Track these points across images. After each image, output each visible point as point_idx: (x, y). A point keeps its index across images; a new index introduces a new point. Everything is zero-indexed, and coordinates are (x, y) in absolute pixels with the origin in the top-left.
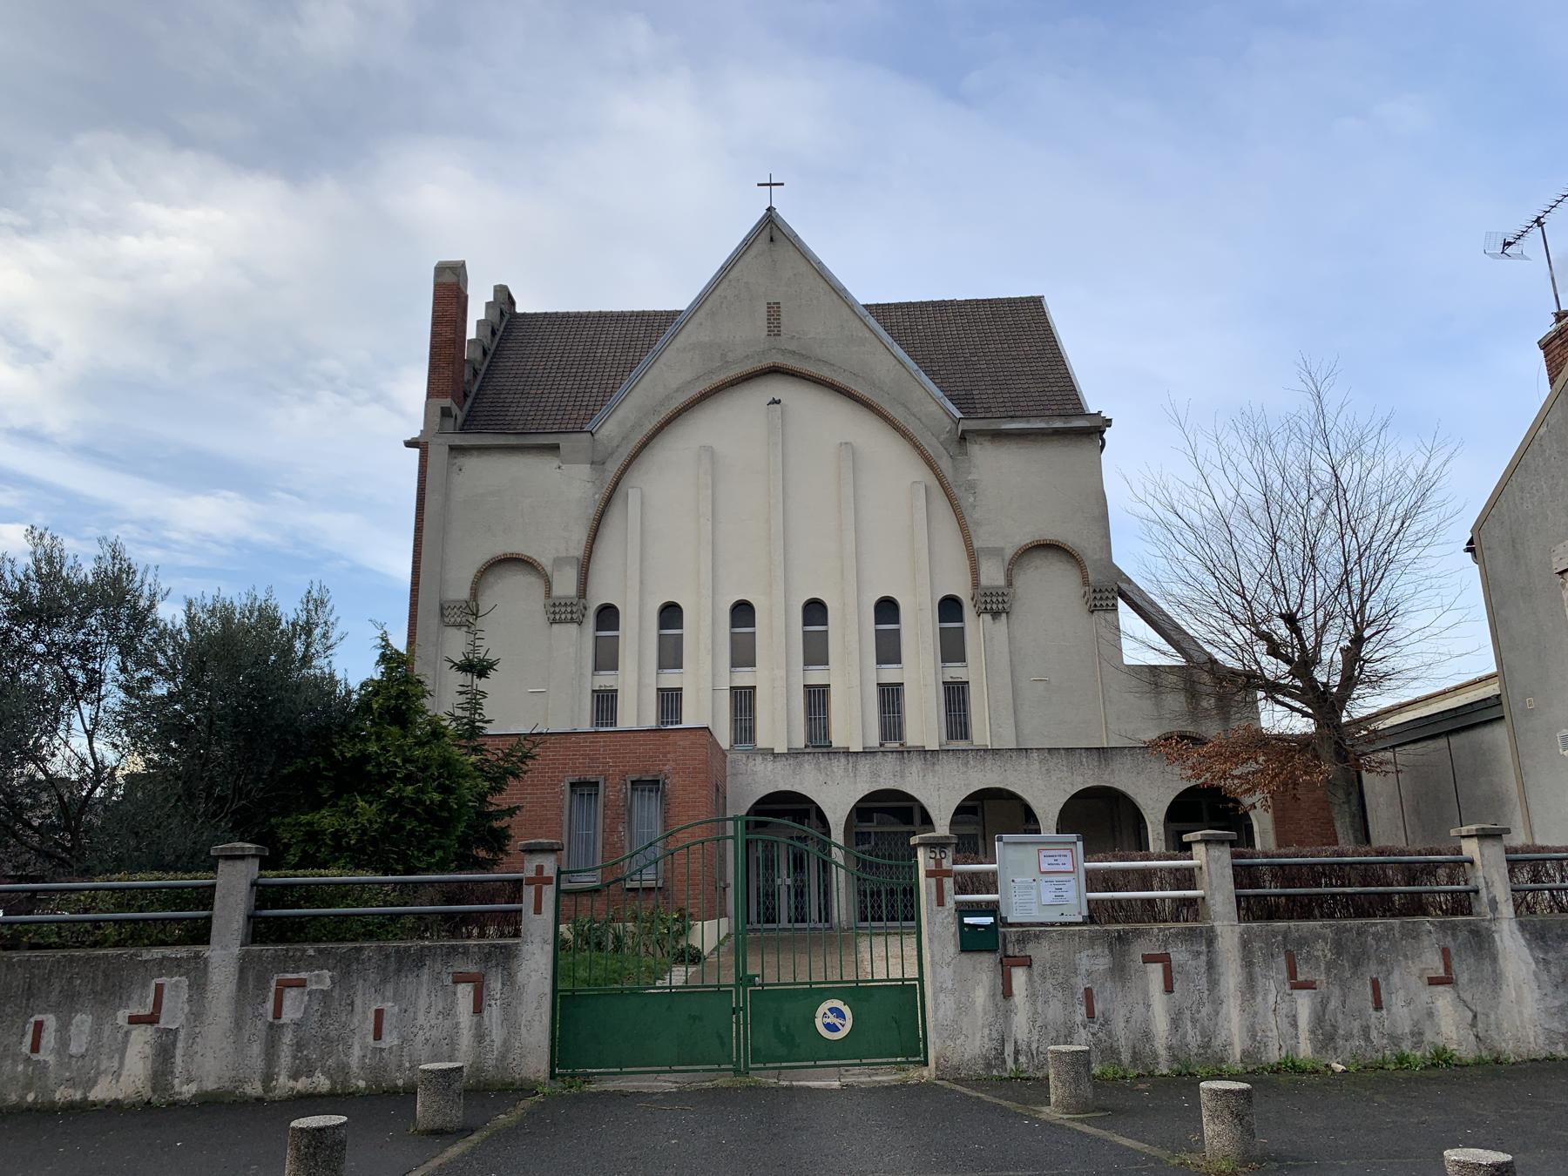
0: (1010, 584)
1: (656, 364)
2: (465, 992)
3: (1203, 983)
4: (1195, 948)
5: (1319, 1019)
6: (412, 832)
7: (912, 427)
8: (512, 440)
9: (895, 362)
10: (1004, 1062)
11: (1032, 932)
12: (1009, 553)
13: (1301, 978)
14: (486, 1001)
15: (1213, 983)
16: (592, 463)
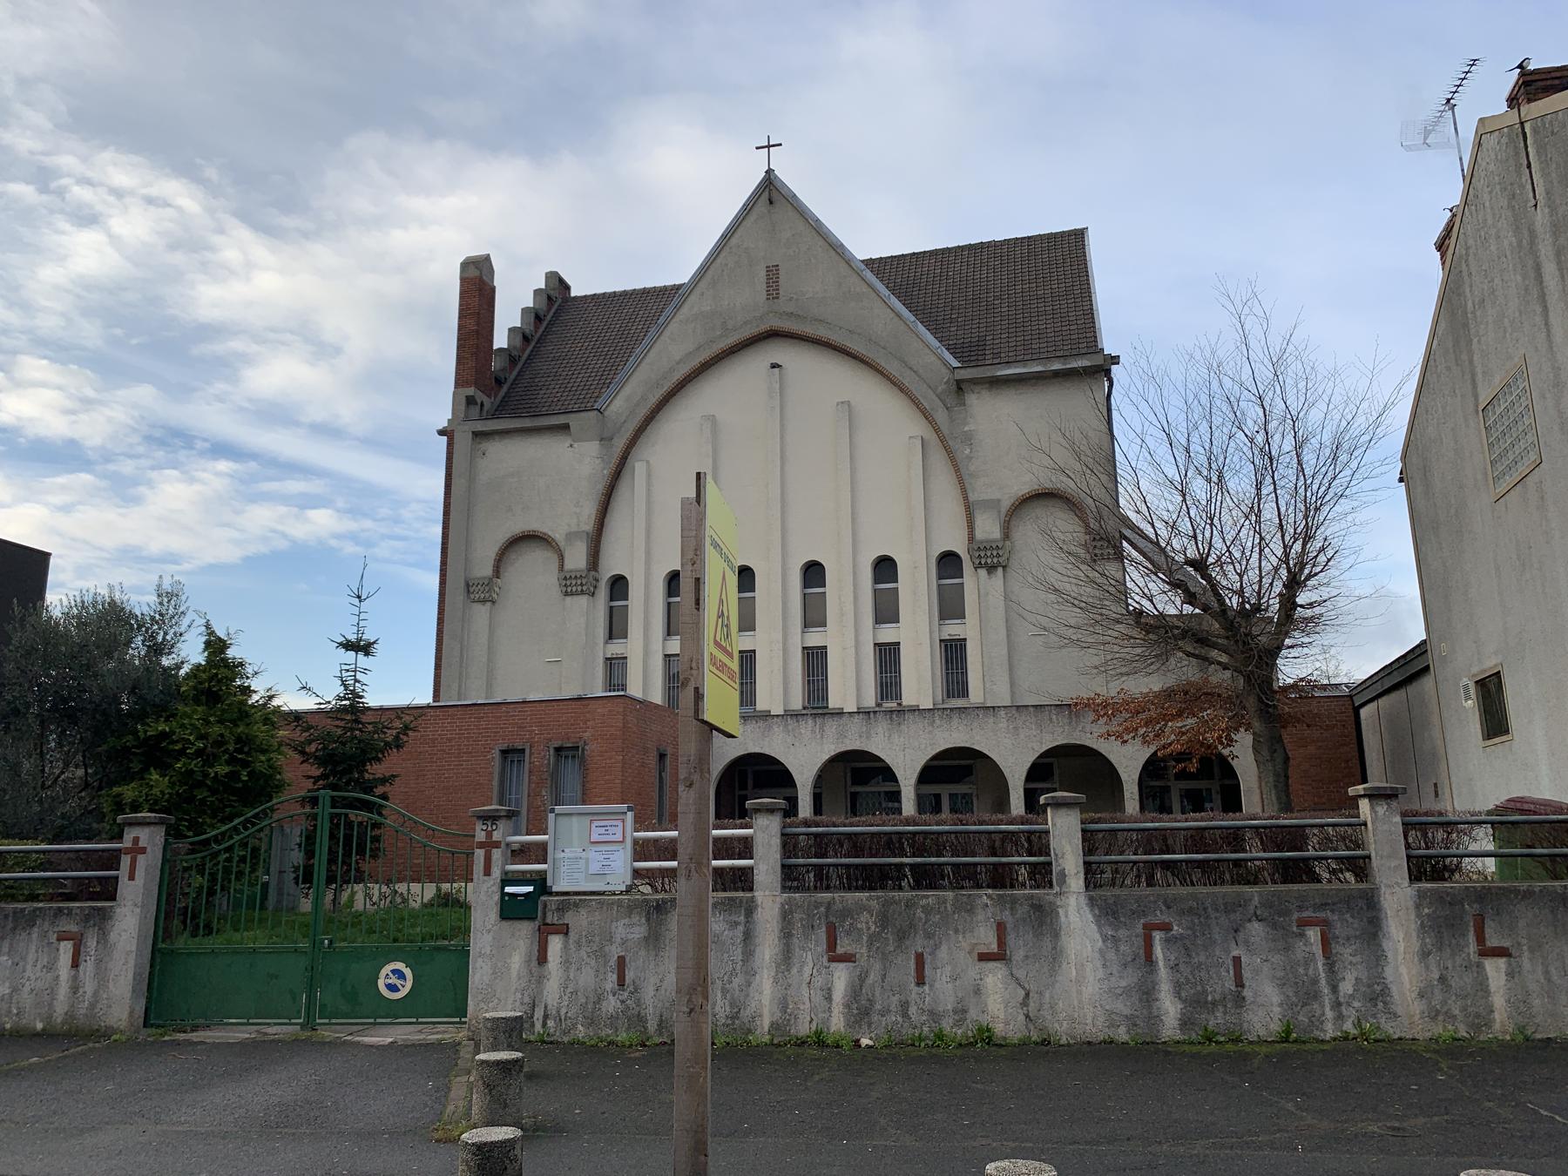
0: (1006, 535)
1: (662, 338)
2: (66, 948)
3: (738, 954)
4: (734, 918)
5: (855, 992)
6: (203, 801)
7: (908, 380)
8: (528, 423)
9: (893, 315)
10: (533, 1025)
11: (574, 900)
12: (1006, 504)
13: (840, 950)
14: (82, 958)
15: (748, 954)
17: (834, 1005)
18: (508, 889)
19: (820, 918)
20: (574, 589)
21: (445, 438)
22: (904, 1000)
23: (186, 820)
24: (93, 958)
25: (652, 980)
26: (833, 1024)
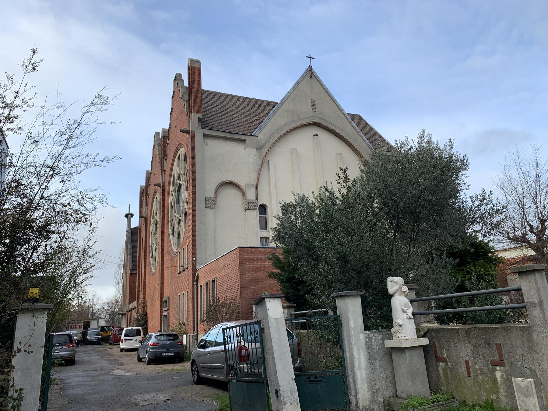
9: (352, 127)
16: (257, 149)
20: (252, 207)
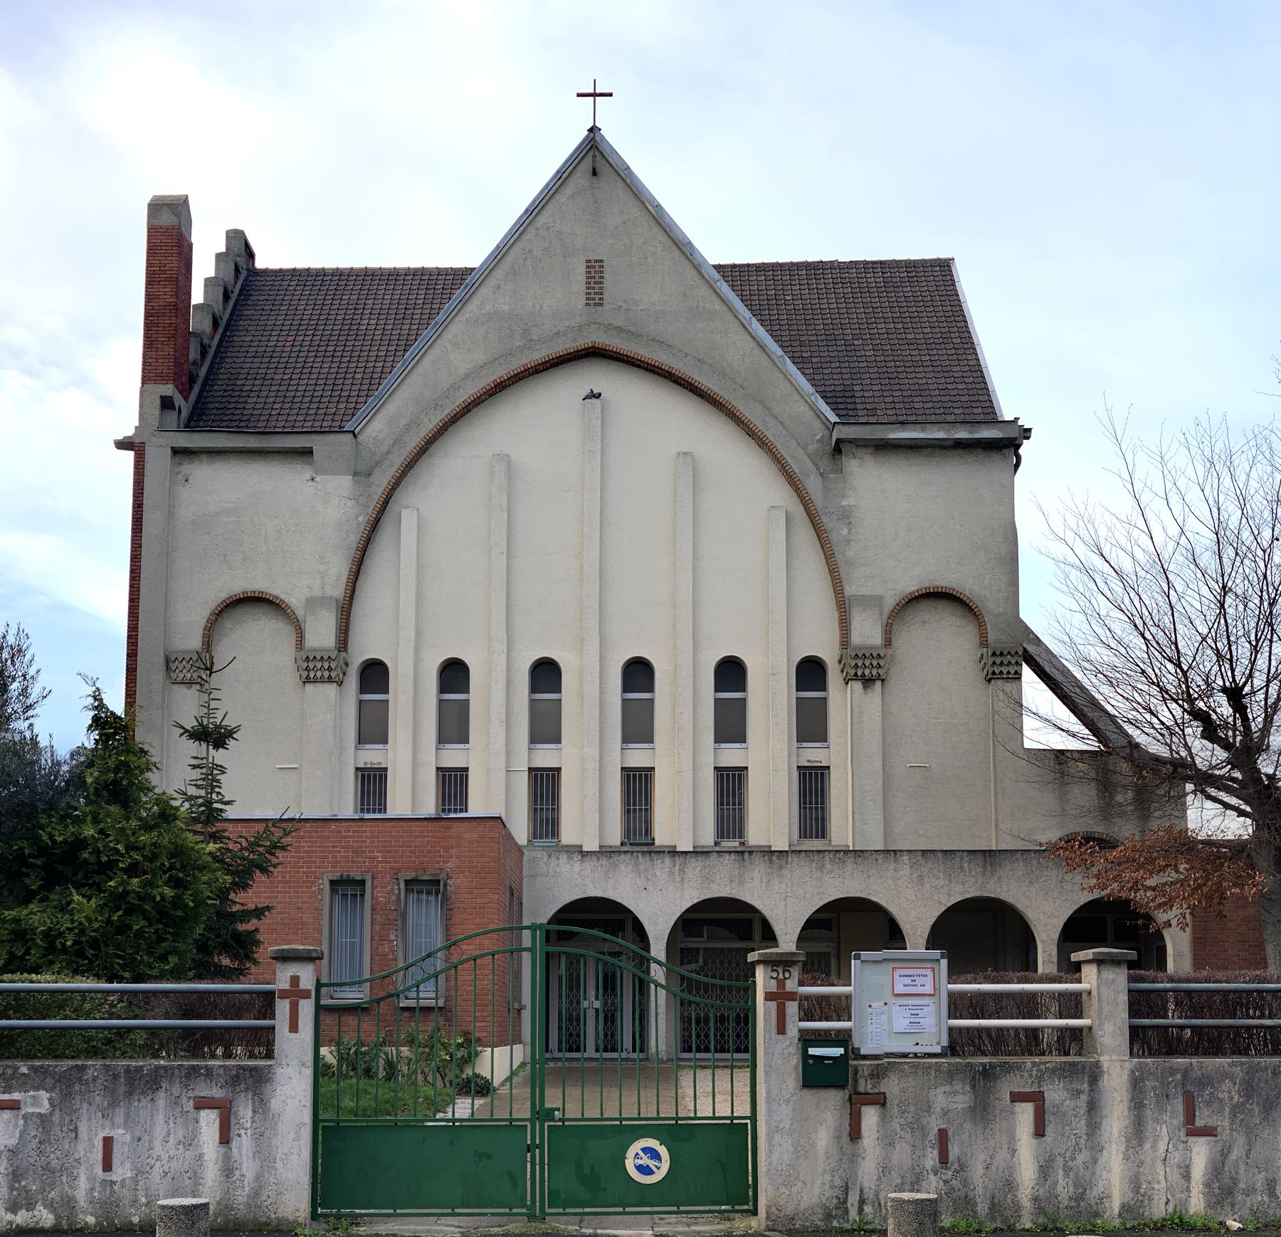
0: (888, 642)
2: (209, 1121)
3: (1081, 1126)
4: (1076, 1086)
5: (1217, 1169)
6: (139, 934)
7: (772, 433)
8: (252, 442)
10: (846, 1212)
11: (885, 1064)
12: (890, 603)
13: (1199, 1123)
14: (234, 1132)
15: (1094, 1126)
16: (355, 474)
17: (1193, 1183)
18: (812, 1051)
19: (1175, 1087)
20: (319, 674)
21: (129, 456)
22: (1271, 1178)
23: (119, 957)
24: (249, 1134)
25: (982, 1157)
26: (1193, 1206)
